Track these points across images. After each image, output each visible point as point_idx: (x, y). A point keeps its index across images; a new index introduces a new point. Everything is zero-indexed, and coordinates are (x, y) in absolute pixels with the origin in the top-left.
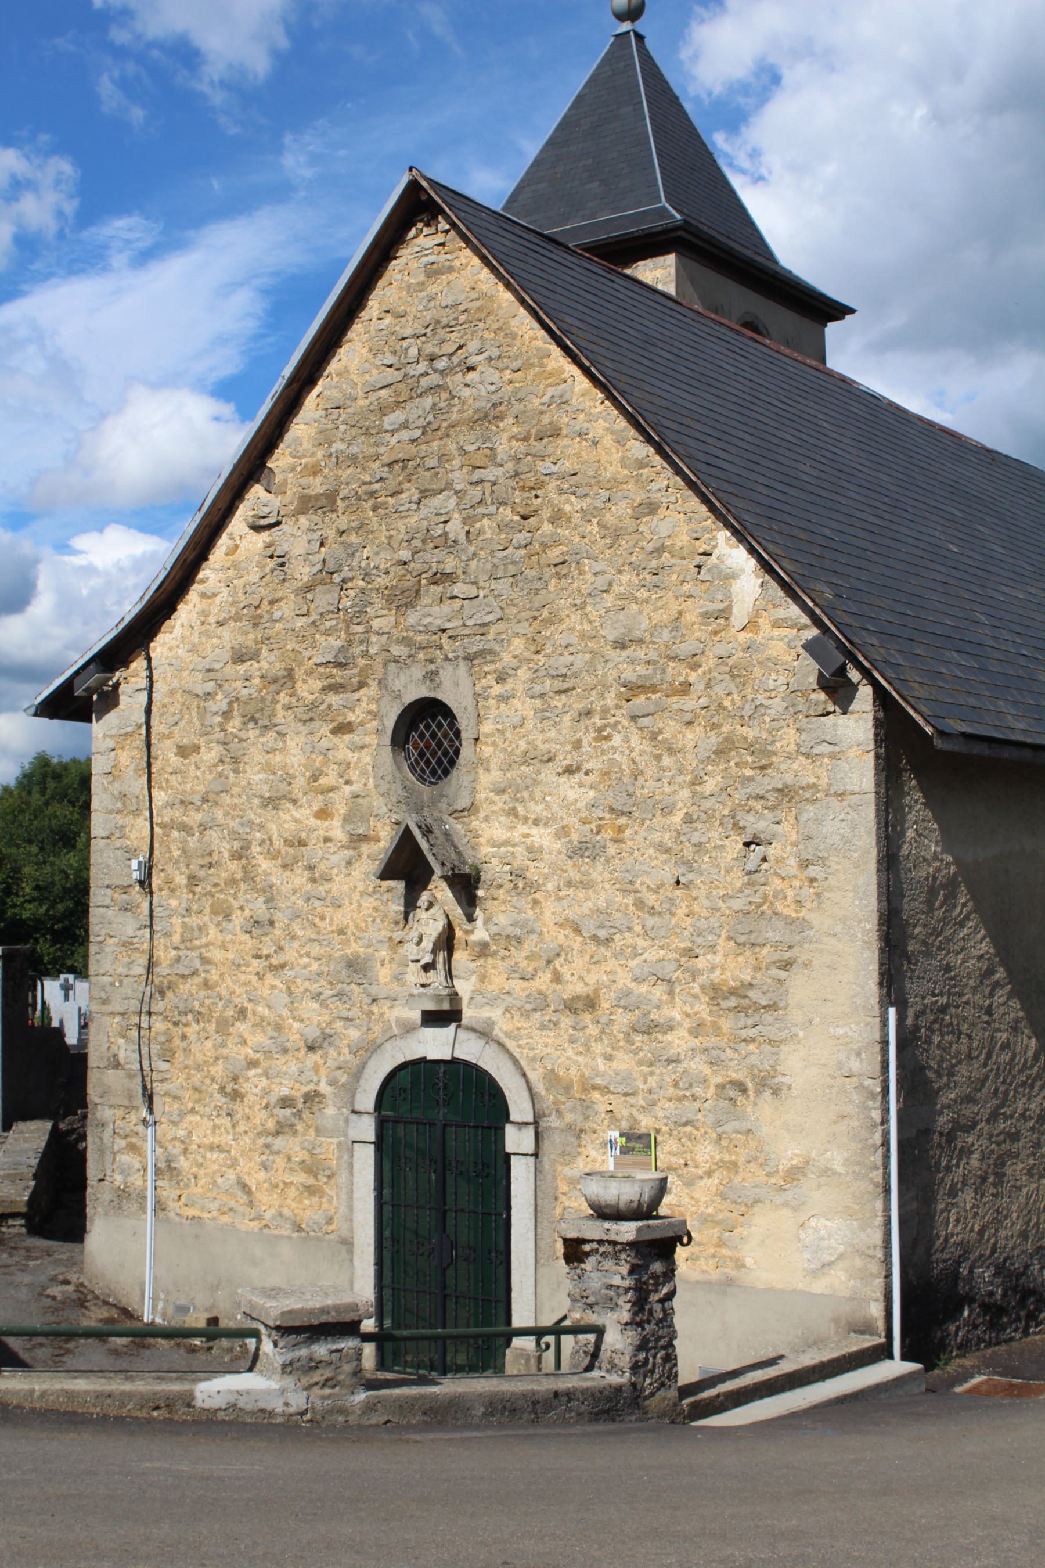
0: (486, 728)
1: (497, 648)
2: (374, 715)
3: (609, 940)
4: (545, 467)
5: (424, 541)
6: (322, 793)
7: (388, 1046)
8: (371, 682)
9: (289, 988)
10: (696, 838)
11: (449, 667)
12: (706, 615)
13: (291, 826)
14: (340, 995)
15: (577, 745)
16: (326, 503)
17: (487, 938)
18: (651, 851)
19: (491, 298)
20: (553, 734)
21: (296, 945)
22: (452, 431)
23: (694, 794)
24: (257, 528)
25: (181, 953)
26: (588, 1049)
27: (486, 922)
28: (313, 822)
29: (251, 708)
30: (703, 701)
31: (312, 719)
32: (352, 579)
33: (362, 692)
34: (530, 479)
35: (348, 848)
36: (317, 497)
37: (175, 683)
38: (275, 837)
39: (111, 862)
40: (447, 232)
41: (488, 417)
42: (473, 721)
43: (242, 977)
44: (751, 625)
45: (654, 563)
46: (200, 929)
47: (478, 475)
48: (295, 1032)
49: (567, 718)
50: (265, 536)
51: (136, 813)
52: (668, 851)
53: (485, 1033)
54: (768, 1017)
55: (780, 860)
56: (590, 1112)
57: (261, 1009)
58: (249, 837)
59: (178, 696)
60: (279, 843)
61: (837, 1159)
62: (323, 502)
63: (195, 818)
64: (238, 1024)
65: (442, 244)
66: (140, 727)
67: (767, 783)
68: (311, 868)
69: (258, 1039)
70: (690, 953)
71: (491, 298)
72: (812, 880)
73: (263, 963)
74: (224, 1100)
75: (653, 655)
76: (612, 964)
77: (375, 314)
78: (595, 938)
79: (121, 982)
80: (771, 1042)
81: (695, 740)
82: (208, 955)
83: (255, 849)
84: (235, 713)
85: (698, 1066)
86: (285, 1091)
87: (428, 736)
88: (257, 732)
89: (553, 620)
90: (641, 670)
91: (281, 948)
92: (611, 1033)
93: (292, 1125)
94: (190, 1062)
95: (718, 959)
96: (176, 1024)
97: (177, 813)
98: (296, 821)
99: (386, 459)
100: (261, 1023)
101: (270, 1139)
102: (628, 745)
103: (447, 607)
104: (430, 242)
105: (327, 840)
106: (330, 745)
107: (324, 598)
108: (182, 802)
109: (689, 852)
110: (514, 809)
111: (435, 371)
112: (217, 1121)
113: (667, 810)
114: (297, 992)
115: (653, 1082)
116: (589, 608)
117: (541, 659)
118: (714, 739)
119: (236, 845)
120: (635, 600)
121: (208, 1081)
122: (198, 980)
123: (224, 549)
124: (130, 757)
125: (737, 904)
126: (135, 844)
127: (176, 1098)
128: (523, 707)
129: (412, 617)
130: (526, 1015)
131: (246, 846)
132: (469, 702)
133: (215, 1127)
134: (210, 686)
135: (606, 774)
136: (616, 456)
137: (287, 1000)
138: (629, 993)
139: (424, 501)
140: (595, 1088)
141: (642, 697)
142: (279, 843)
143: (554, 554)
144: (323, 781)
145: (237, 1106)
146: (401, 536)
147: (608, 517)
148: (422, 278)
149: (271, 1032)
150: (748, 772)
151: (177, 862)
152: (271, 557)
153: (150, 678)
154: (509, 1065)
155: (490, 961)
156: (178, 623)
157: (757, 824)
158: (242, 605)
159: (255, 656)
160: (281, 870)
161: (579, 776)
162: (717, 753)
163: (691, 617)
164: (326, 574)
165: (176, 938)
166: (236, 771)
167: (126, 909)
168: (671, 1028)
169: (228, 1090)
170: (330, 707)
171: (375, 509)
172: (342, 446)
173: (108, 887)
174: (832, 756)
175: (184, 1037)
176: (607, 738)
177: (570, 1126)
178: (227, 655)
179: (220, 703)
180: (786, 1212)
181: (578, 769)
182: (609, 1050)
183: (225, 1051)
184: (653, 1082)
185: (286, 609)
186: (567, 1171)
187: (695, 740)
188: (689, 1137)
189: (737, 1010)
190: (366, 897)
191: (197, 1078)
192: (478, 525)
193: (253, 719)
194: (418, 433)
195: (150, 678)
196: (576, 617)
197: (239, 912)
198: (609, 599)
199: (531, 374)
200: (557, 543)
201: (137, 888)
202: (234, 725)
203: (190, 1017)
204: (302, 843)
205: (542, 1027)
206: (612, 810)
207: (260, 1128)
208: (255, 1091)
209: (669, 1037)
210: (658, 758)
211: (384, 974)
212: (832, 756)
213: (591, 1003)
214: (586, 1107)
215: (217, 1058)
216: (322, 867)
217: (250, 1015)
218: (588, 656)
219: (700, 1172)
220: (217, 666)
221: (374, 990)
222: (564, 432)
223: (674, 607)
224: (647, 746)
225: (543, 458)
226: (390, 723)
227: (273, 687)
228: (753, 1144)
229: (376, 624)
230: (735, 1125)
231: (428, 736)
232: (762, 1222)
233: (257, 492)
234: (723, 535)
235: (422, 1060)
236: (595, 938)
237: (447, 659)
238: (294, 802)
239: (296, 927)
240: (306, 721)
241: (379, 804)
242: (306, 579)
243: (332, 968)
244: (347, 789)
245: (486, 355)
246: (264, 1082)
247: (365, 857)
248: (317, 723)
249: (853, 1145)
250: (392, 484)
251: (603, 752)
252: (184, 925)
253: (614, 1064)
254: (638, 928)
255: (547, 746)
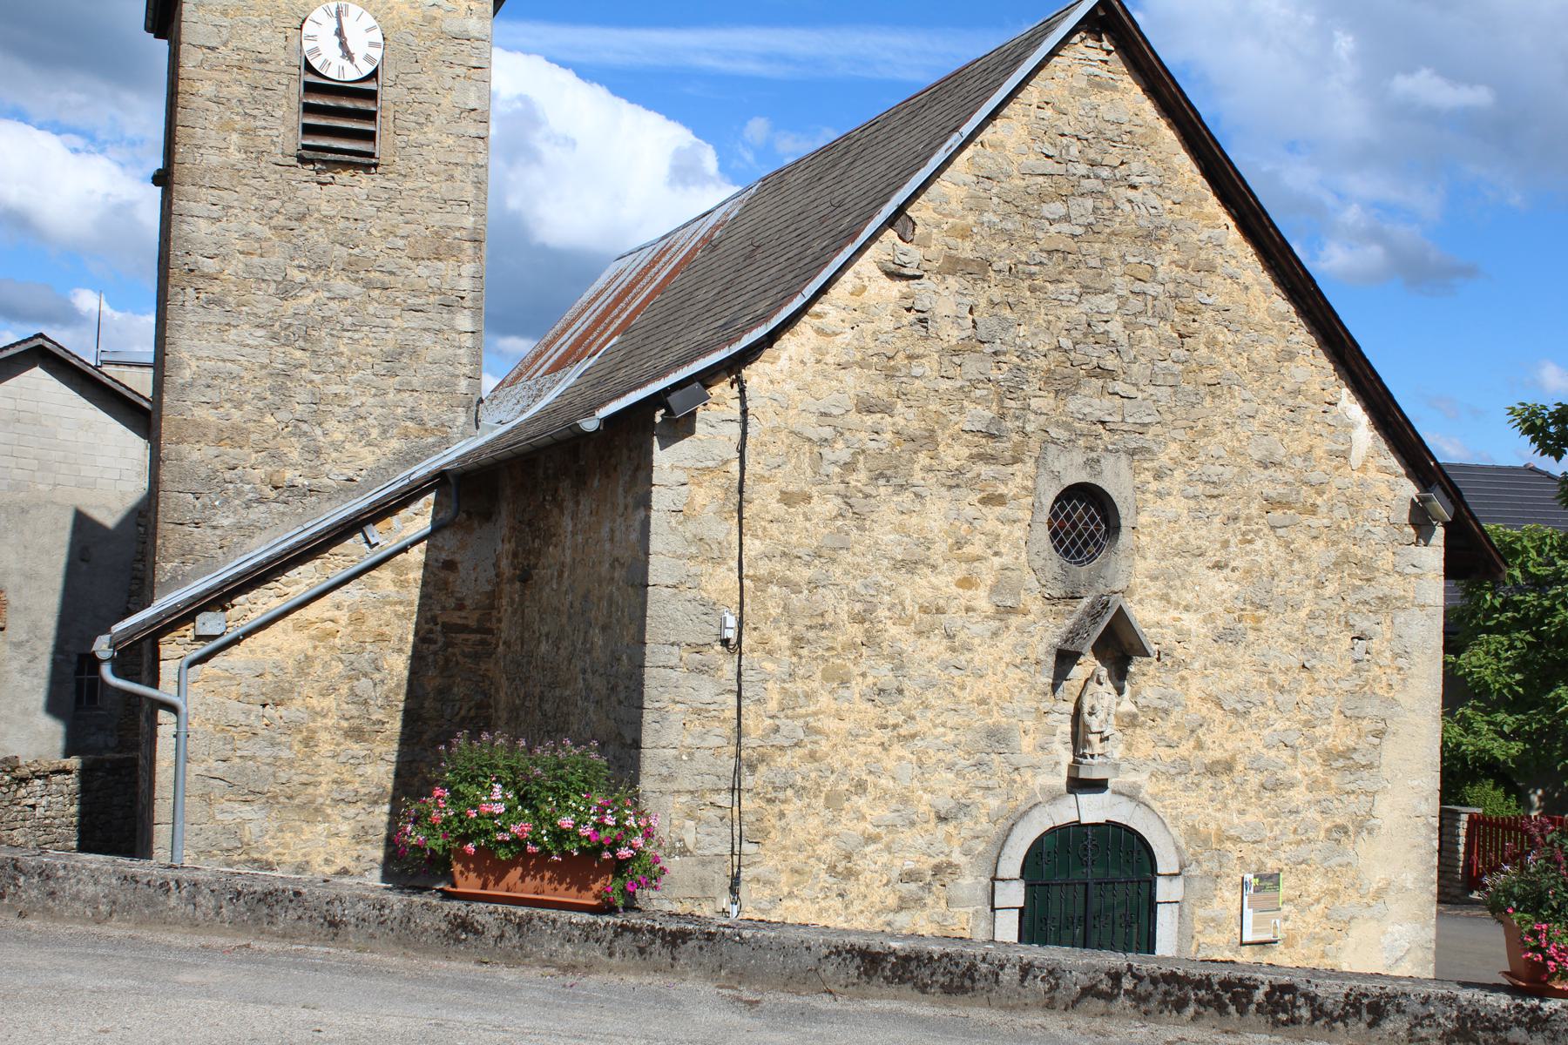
0: (1144, 519)
1: (1155, 448)
2: (1030, 491)
3: (1247, 713)
4: (1200, 296)
5: (1085, 335)
6: (967, 562)
7: (1035, 813)
8: (1027, 459)
9: (919, 759)
10: (1318, 631)
11: (1111, 459)
12: (1331, 453)
13: (929, 594)
14: (978, 764)
15: (1225, 544)
16: (977, 269)
17: (1134, 709)
18: (1282, 640)
19: (1155, 130)
20: (1203, 532)
21: (930, 714)
22: (1114, 238)
23: (1317, 595)
24: (893, 275)
25: (777, 722)
26: (1226, 806)
27: (1135, 694)
28: (954, 590)
29: (881, 463)
30: (1326, 522)
31: (958, 486)
32: (1005, 353)
33: (1016, 466)
34: (1190, 304)
35: (994, 618)
36: (967, 262)
37: (778, 421)
38: (908, 603)
39: (679, 615)
40: (1109, 53)
41: (1151, 237)
42: (1132, 511)
43: (861, 748)
44: (1364, 468)
45: (1290, 402)
46: (807, 696)
47: (1138, 286)
48: (924, 803)
49: (1217, 520)
50: (900, 286)
51: (718, 561)
52: (1296, 640)
53: (1132, 795)
54: (1365, 774)
55: (1379, 653)
56: (1224, 860)
57: (883, 781)
58: (875, 600)
59: (783, 436)
60: (912, 609)
61: (1409, 878)
62: (975, 268)
63: (801, 574)
64: (854, 798)
65: (1106, 62)
66: (726, 462)
67: (1370, 593)
68: (950, 637)
69: (883, 813)
70: (1307, 723)
71: (1155, 130)
72: (1400, 669)
73: (889, 733)
74: (832, 880)
75: (1290, 478)
76: (1249, 732)
77: (1035, 102)
78: (1235, 712)
79: (690, 755)
80: (1366, 793)
81: (1319, 553)
82: (819, 724)
83: (882, 613)
84: (860, 465)
85: (1312, 814)
86: (909, 865)
87: (1084, 520)
88: (890, 489)
89: (1207, 432)
90: (1281, 489)
91: (913, 718)
92: (1244, 792)
93: (921, 899)
94: (788, 843)
95: (1331, 729)
96: (770, 801)
97: (779, 567)
98: (934, 588)
99: (1044, 244)
100: (884, 795)
101: (891, 916)
102: (1266, 550)
103: (1107, 402)
104: (1092, 54)
105: (968, 610)
106: (978, 515)
107: (973, 366)
108: (784, 554)
109: (1312, 642)
110: (1167, 594)
111: (1097, 177)
112: (823, 904)
113: (1295, 608)
114: (930, 762)
115: (1277, 831)
116: (1237, 429)
117: (1195, 466)
118: (1333, 554)
119: (858, 607)
120: (1277, 430)
121: (812, 861)
122: (800, 752)
123: (849, 287)
124: (707, 497)
125: (1346, 685)
126: (714, 596)
127: (767, 883)
128: (1177, 505)
129: (1074, 404)
130: (1172, 778)
131: (871, 609)
132: (1129, 492)
133: (821, 910)
134: (827, 432)
135: (1248, 572)
136: (1264, 305)
137: (917, 771)
138: (1258, 757)
139: (1085, 297)
140: (1228, 838)
141: (1280, 512)
142: (912, 609)
143: (1208, 375)
144: (967, 549)
145: (853, 888)
146: (1060, 325)
147: (1254, 355)
148: (1084, 84)
149: (894, 804)
150: (1358, 583)
151: (776, 621)
152: (908, 310)
153: (744, 412)
154: (1158, 823)
155: (1138, 731)
156: (784, 356)
157: (1362, 624)
158: (870, 352)
159: (887, 410)
160: (913, 638)
161: (1227, 571)
162: (1335, 564)
163: (1318, 452)
164: (976, 342)
165: (772, 706)
166: (861, 528)
167: (701, 670)
168: (1293, 785)
169: (839, 869)
170: (979, 475)
171: (1032, 290)
172: (996, 219)
173: (672, 644)
174: (1418, 576)
175: (782, 815)
176: (1250, 542)
177: (1207, 875)
178: (851, 404)
179: (841, 452)
180: (1373, 923)
181: (1226, 565)
182: (1243, 806)
183: (837, 828)
184: (1277, 831)
185: (928, 367)
186: (1200, 912)
187: (1319, 553)
188: (1304, 872)
189: (1344, 768)
190: (1012, 668)
191: (797, 860)
192: (1139, 332)
193: (881, 475)
194: (1079, 230)
195: (744, 412)
196: (1225, 435)
197: (860, 679)
198: (1255, 425)
199: (1188, 212)
200: (1212, 366)
201: (718, 647)
202: (859, 478)
203: (790, 792)
204: (940, 611)
205: (1186, 788)
206: (1252, 603)
207: (878, 906)
208: (873, 867)
209: (1291, 793)
210: (1291, 563)
211: (1026, 743)
212: (1418, 576)
213: (1229, 767)
214: (1221, 855)
215: (826, 836)
216: (962, 636)
217: (870, 789)
218: (1236, 470)
219: (1310, 900)
220: (835, 411)
221: (1014, 759)
222: (1219, 271)
223: (1307, 442)
224: (1281, 552)
225: (1200, 288)
226: (1048, 500)
227: (910, 445)
228: (1351, 873)
229: (1034, 403)
230: (1339, 860)
231: (1084, 520)
232: (1356, 932)
233: (891, 234)
234: (1346, 391)
235: (1078, 825)
236: (1235, 712)
237: (1106, 449)
238: (934, 567)
239: (930, 696)
240: (951, 487)
241: (1031, 580)
242: (954, 342)
243: (969, 737)
244: (996, 560)
245: (1147, 179)
246: (885, 857)
247: (1012, 628)
248: (964, 491)
249: (1421, 867)
250: (1052, 269)
251: (1247, 553)
252: (784, 691)
253: (1248, 818)
254: (1270, 703)
255: (1199, 542)
